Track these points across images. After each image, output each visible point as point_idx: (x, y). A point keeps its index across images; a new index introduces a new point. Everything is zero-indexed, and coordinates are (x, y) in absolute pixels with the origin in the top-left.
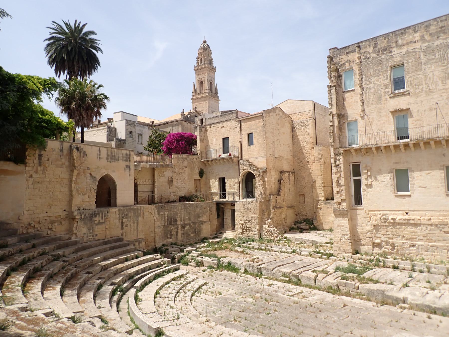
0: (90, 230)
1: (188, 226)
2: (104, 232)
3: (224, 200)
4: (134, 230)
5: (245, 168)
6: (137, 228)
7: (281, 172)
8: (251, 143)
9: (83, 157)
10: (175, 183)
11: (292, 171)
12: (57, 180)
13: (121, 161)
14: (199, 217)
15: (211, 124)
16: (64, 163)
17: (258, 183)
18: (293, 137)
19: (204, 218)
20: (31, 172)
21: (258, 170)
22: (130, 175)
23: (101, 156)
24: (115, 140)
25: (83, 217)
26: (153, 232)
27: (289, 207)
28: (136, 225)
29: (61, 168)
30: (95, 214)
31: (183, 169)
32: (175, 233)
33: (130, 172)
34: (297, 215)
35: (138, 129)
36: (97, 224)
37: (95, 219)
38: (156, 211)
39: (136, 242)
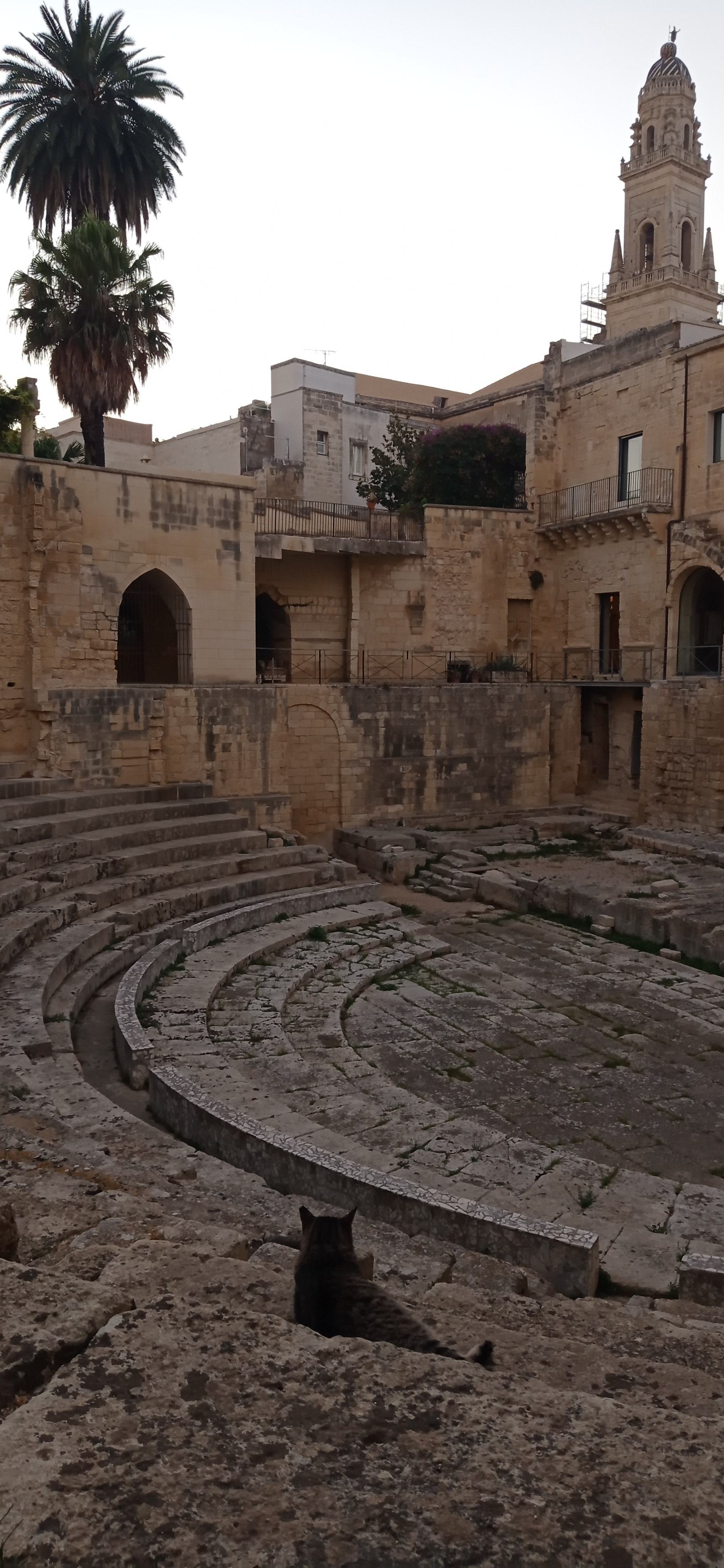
1: (463, 767)
3: (613, 679)
5: (689, 551)
9: (67, 508)
10: (431, 613)
13: (206, 525)
14: (510, 737)
15: (581, 383)
19: (528, 741)
22: (238, 577)
23: (131, 508)
24: (267, 466)
25: (68, 708)
26: (335, 779)
28: (258, 746)
30: (110, 701)
31: (464, 561)
32: (412, 785)
33: (237, 566)
35: (352, 423)
36: (119, 736)
37: (112, 718)
38: (345, 708)
39: (261, 802)
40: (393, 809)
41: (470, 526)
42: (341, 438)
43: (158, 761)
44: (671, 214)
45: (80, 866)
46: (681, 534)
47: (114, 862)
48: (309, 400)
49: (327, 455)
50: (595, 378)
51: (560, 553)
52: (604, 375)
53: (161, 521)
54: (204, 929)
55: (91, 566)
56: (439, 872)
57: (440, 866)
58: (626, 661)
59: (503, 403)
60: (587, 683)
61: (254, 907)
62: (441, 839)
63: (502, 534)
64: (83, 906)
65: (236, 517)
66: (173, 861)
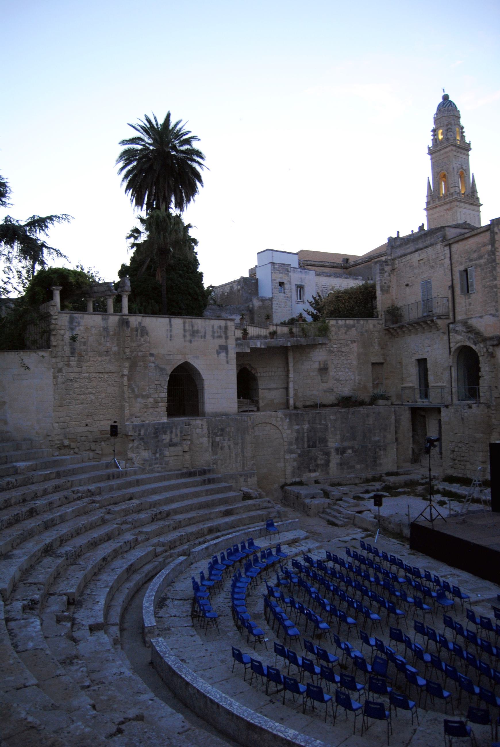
0: (155, 453)
4: (237, 455)
5: (459, 338)
6: (243, 452)
8: (467, 289)
9: (142, 336)
10: (332, 372)
12: (101, 376)
15: (401, 257)
16: (111, 348)
17: (484, 367)
20: (60, 365)
21: (485, 340)
22: (227, 362)
29: (106, 356)
30: (163, 427)
37: (164, 436)
39: (241, 475)
40: (313, 475)
41: (348, 328)
42: (290, 284)
43: (187, 457)
44: (453, 168)
45: (142, 516)
46: (454, 330)
47: (160, 512)
48: (274, 268)
49: (284, 293)
50: (408, 254)
51: (396, 339)
52: (411, 253)
53: (188, 338)
54: (202, 549)
55: (154, 362)
56: (334, 510)
57: (336, 507)
58: (432, 394)
59: (376, 260)
61: (230, 536)
62: (336, 492)
64: (140, 538)
65: (226, 333)
66: (191, 510)
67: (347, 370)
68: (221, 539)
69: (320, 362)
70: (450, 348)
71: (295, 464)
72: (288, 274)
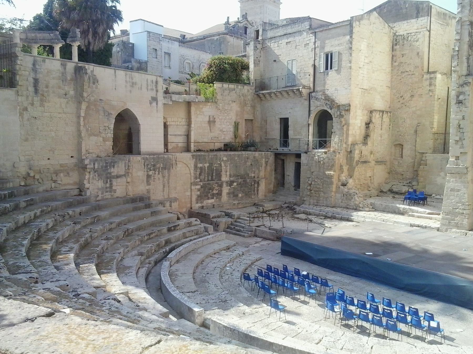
2: (124, 187)
3: (286, 150)
7: (371, 112)
10: (218, 125)
11: (388, 109)
12: (60, 115)
18: (392, 59)
26: (189, 190)
27: (378, 162)
34: (389, 173)
37: (112, 170)
40: (211, 201)
41: (231, 90)
42: (161, 52)
46: (315, 97)
47: (128, 230)
48: (149, 36)
49: (157, 58)
59: (209, 38)
60: (277, 152)
63: (243, 95)
67: (228, 124)
68: (181, 248)
69: (210, 116)
70: (309, 111)
71: (199, 193)
72: (160, 42)
